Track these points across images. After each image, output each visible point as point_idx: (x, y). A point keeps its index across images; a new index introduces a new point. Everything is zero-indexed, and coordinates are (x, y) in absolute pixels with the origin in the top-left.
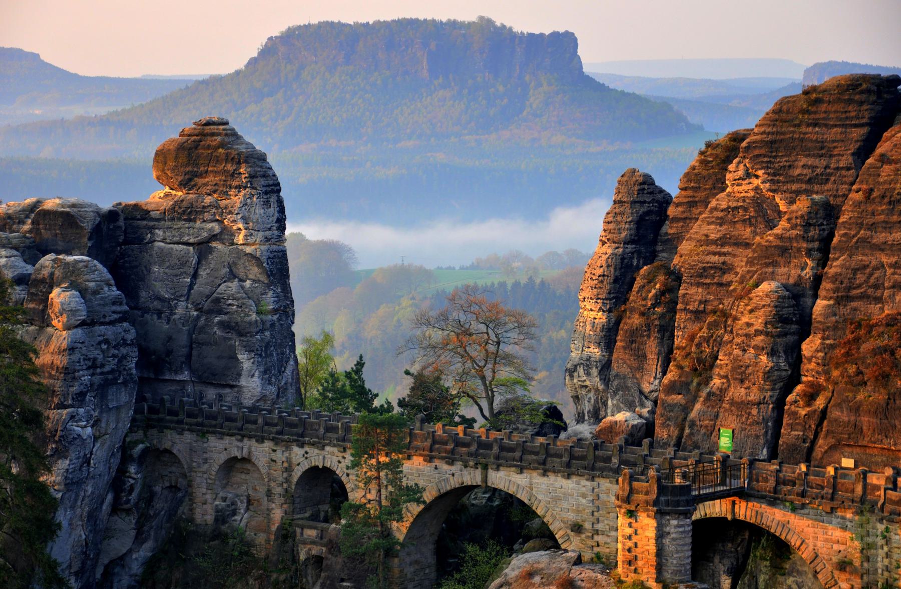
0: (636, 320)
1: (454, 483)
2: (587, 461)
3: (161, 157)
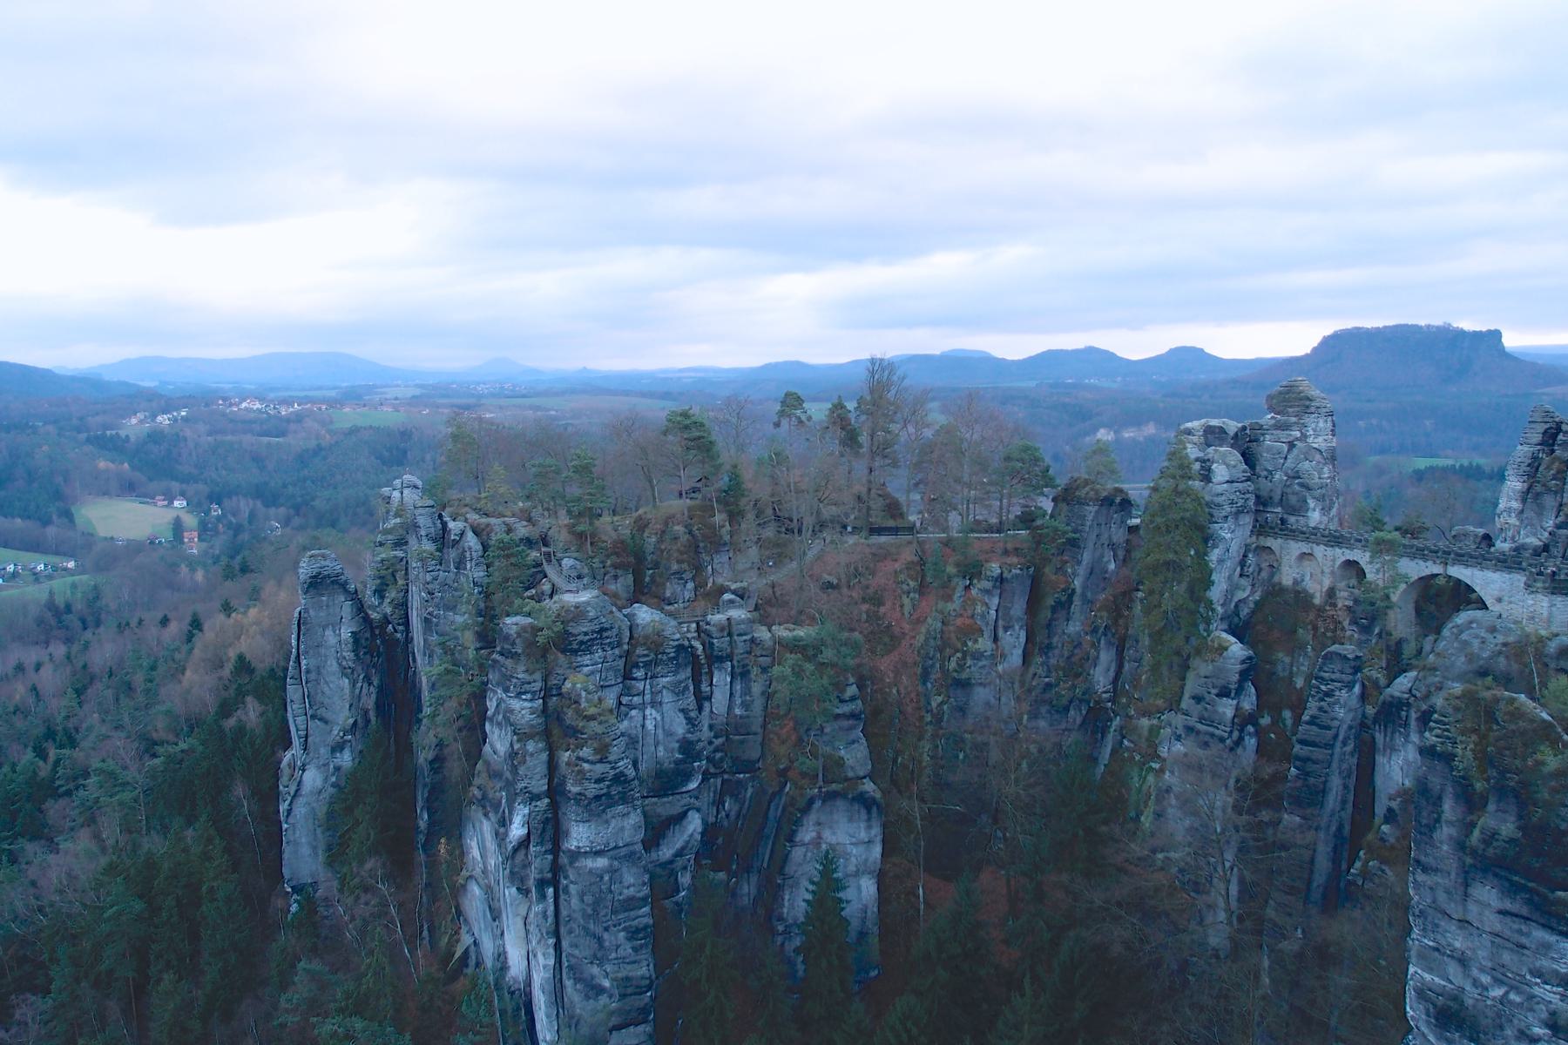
0: (1538, 488)
1: (1427, 572)
2: (1507, 563)
3: (1270, 398)
